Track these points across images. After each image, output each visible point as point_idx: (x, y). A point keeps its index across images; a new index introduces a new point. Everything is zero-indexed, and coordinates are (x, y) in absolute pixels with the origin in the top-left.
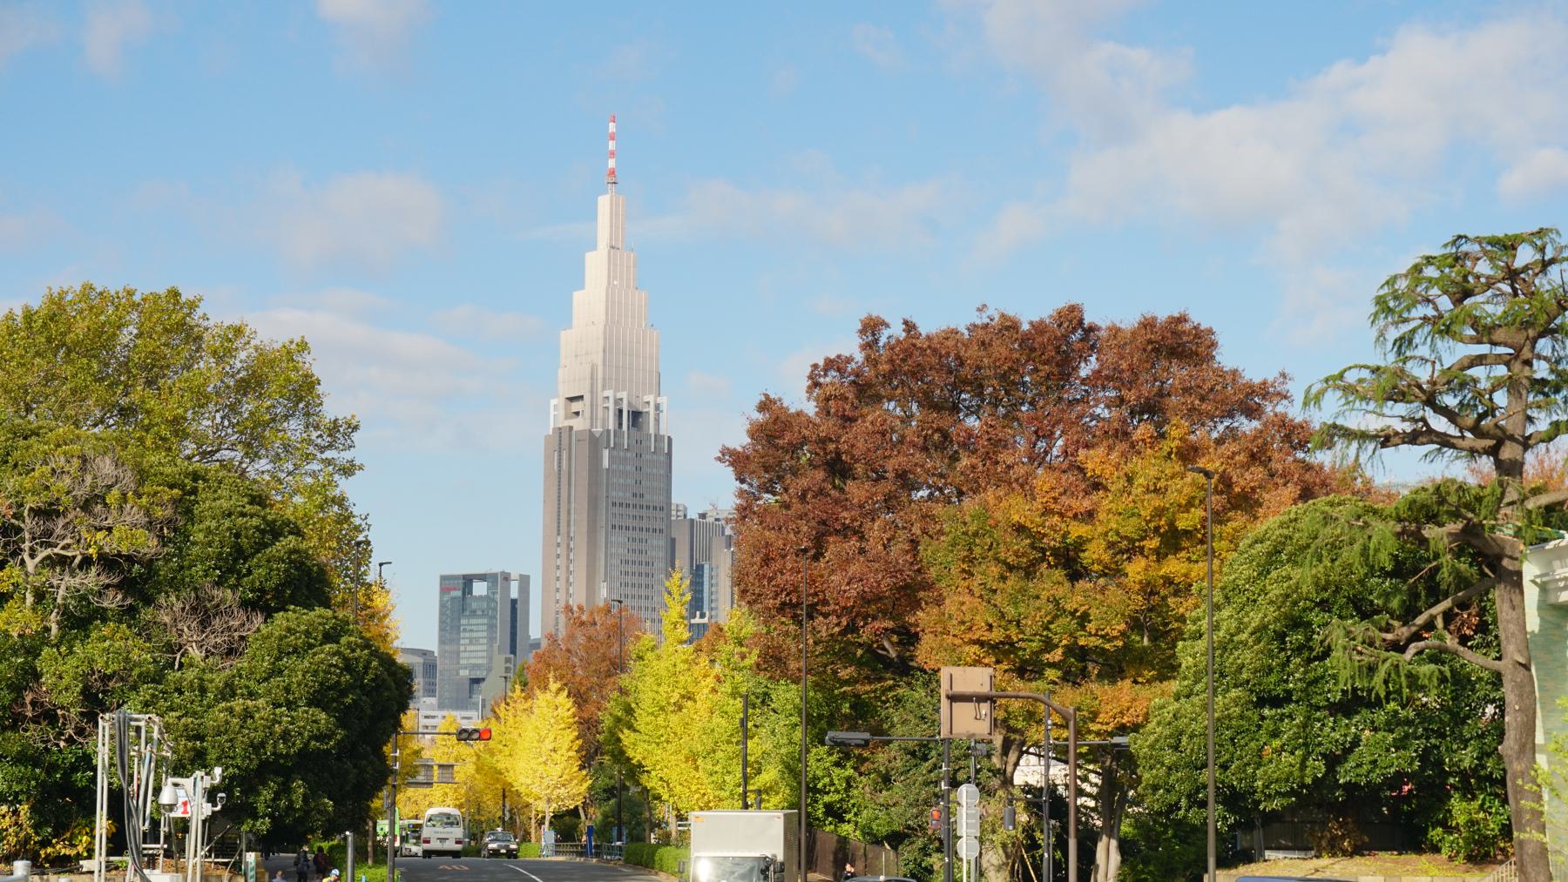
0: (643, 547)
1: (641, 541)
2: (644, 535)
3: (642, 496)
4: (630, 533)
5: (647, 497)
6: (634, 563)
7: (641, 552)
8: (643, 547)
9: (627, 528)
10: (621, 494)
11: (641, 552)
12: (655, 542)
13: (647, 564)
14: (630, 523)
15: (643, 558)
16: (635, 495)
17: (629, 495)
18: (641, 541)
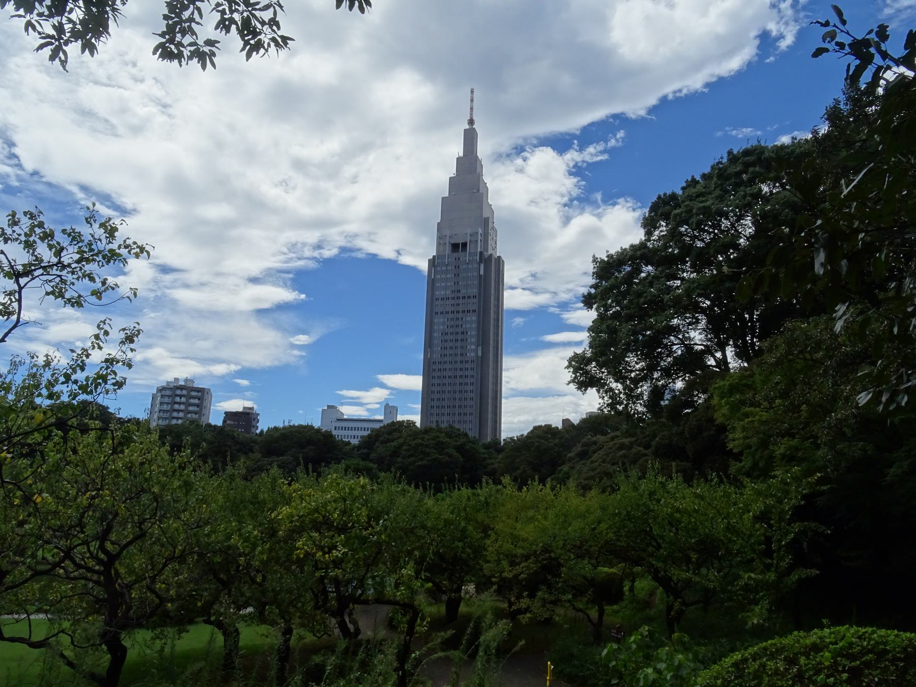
0: (460, 323)
1: (458, 319)
2: (460, 315)
3: (459, 291)
4: (451, 316)
5: (463, 291)
6: (452, 333)
7: (457, 326)
8: (460, 323)
9: (447, 313)
10: (443, 293)
11: (457, 326)
12: (469, 319)
13: (463, 333)
14: (449, 309)
15: (459, 330)
16: (453, 292)
17: (448, 292)
18: (458, 319)
